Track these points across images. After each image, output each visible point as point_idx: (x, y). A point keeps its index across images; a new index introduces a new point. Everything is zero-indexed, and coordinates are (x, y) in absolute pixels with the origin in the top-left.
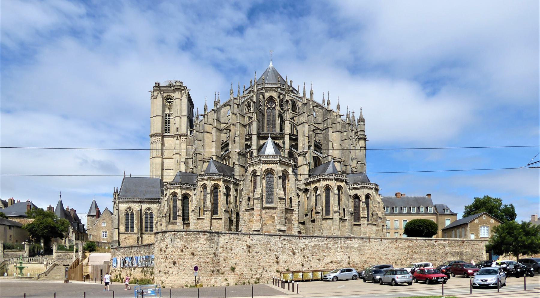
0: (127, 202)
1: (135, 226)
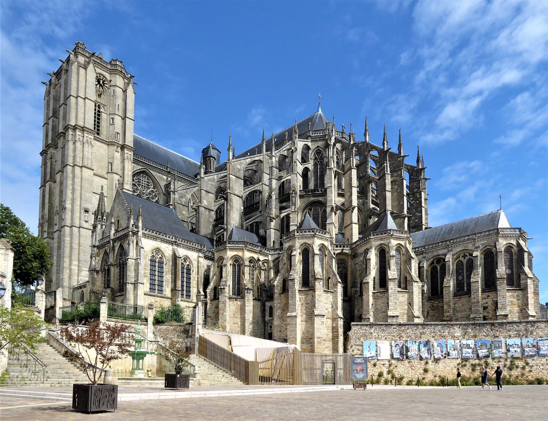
0: (155, 238)
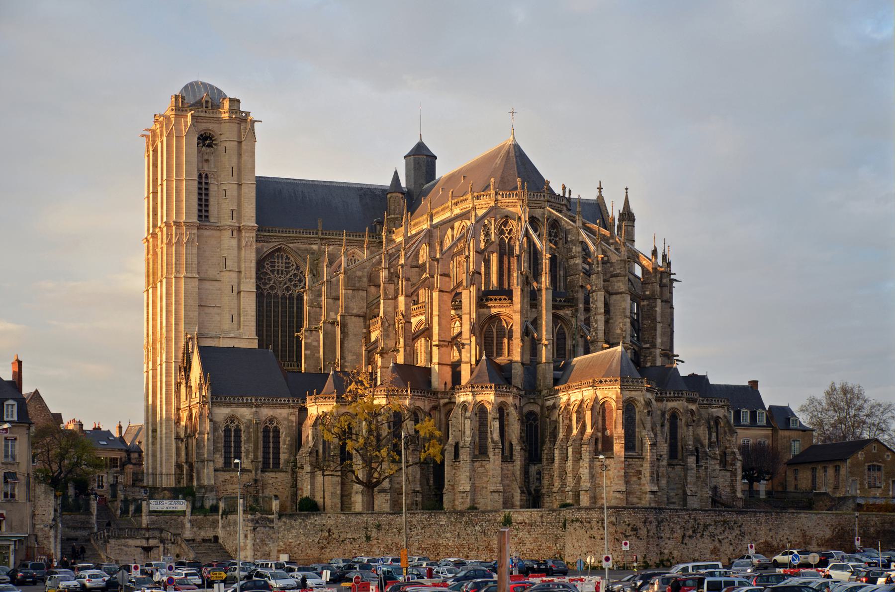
0: (229, 405)
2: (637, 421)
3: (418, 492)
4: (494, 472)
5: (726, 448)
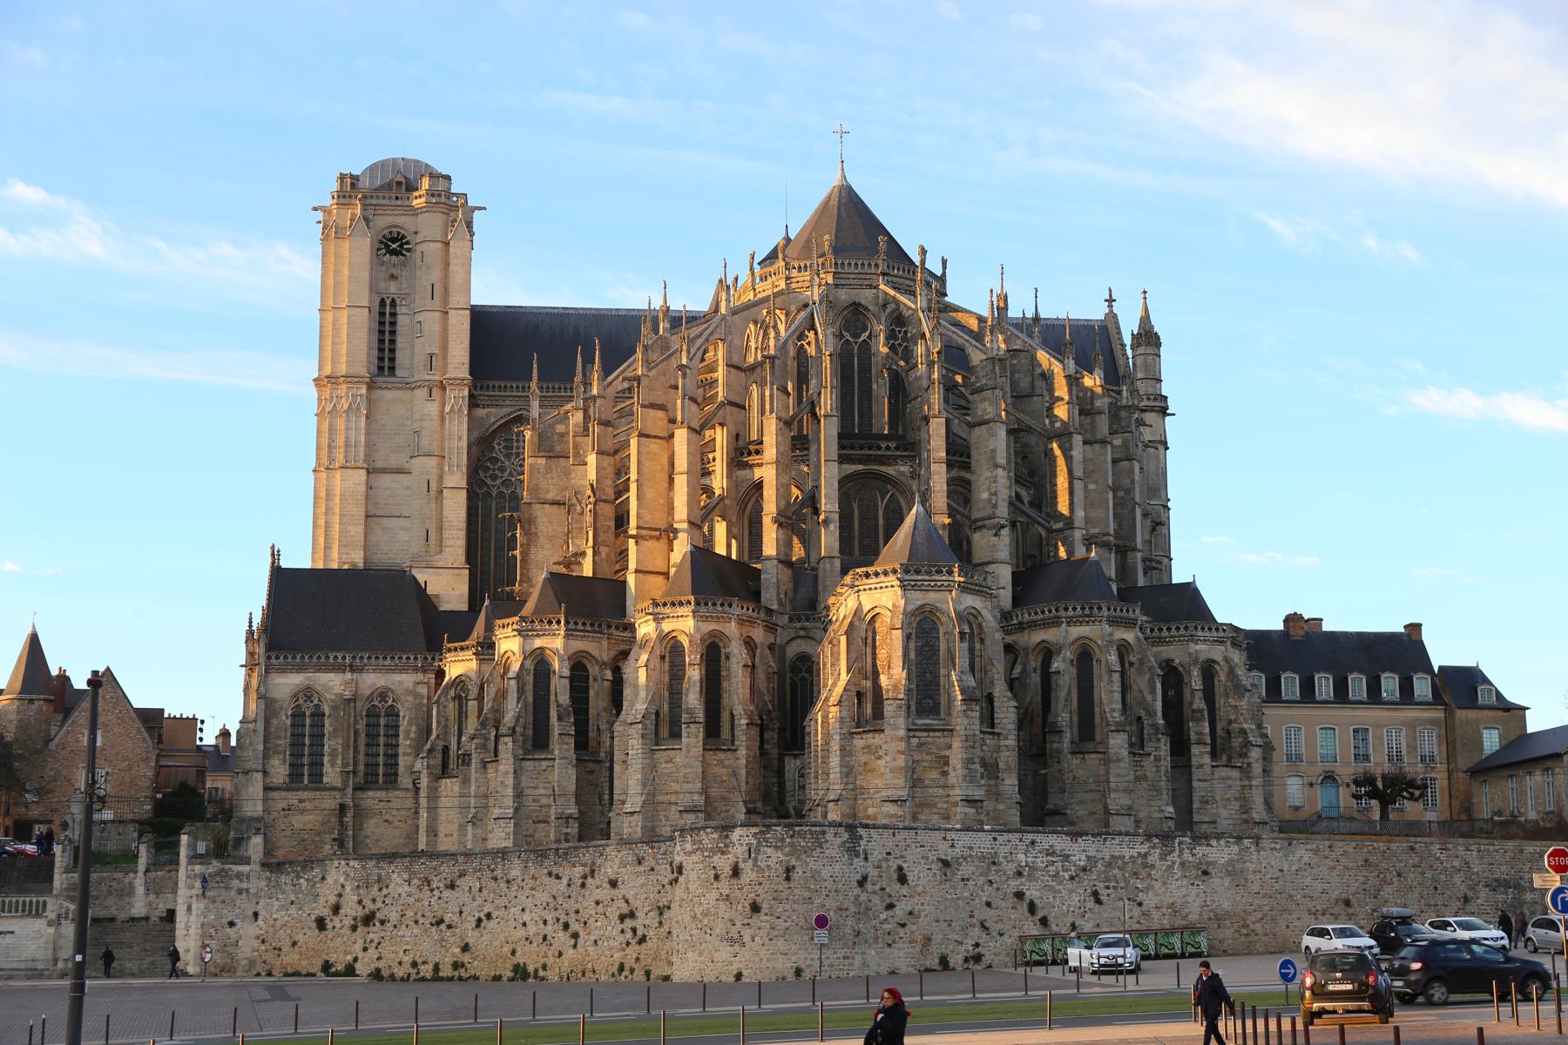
0: (300, 669)
1: (326, 759)
2: (941, 653)
3: (570, 817)
4: (688, 771)
5: (1230, 722)
